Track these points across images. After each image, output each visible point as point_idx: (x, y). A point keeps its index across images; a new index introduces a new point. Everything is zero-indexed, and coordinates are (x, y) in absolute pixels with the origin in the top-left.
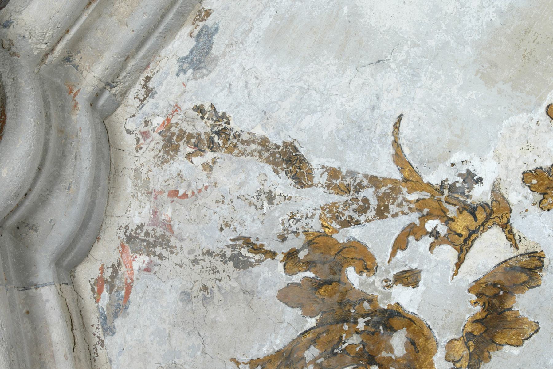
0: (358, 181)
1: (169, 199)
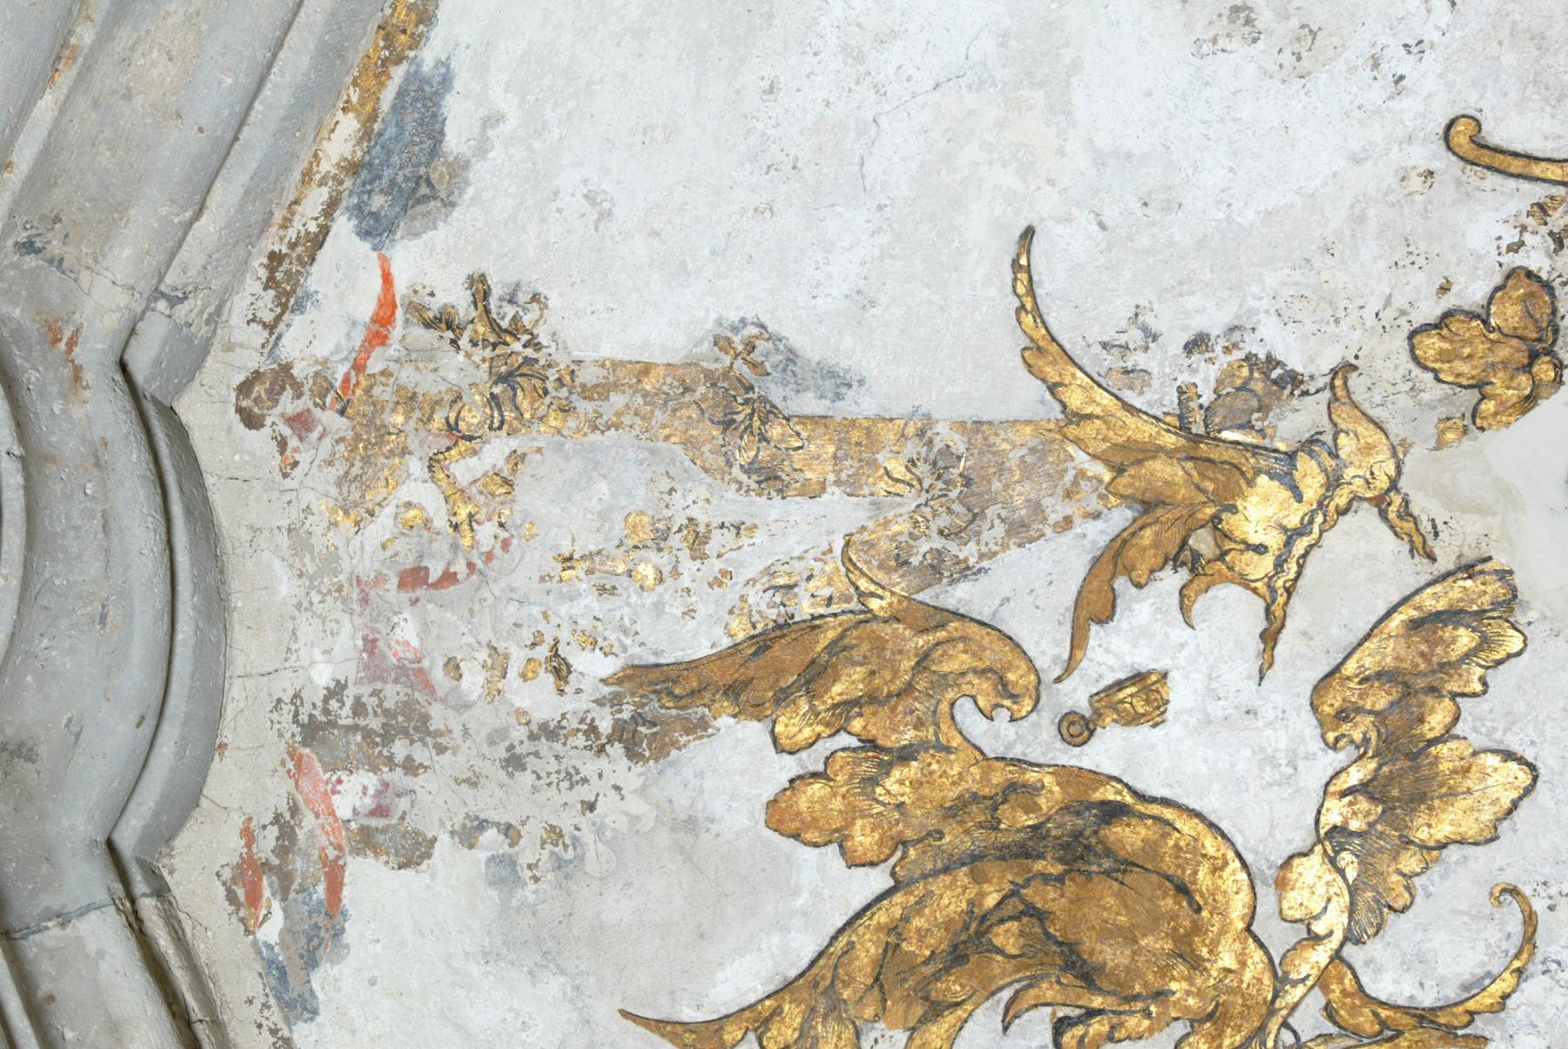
0: (938, 445)
1: (405, 596)
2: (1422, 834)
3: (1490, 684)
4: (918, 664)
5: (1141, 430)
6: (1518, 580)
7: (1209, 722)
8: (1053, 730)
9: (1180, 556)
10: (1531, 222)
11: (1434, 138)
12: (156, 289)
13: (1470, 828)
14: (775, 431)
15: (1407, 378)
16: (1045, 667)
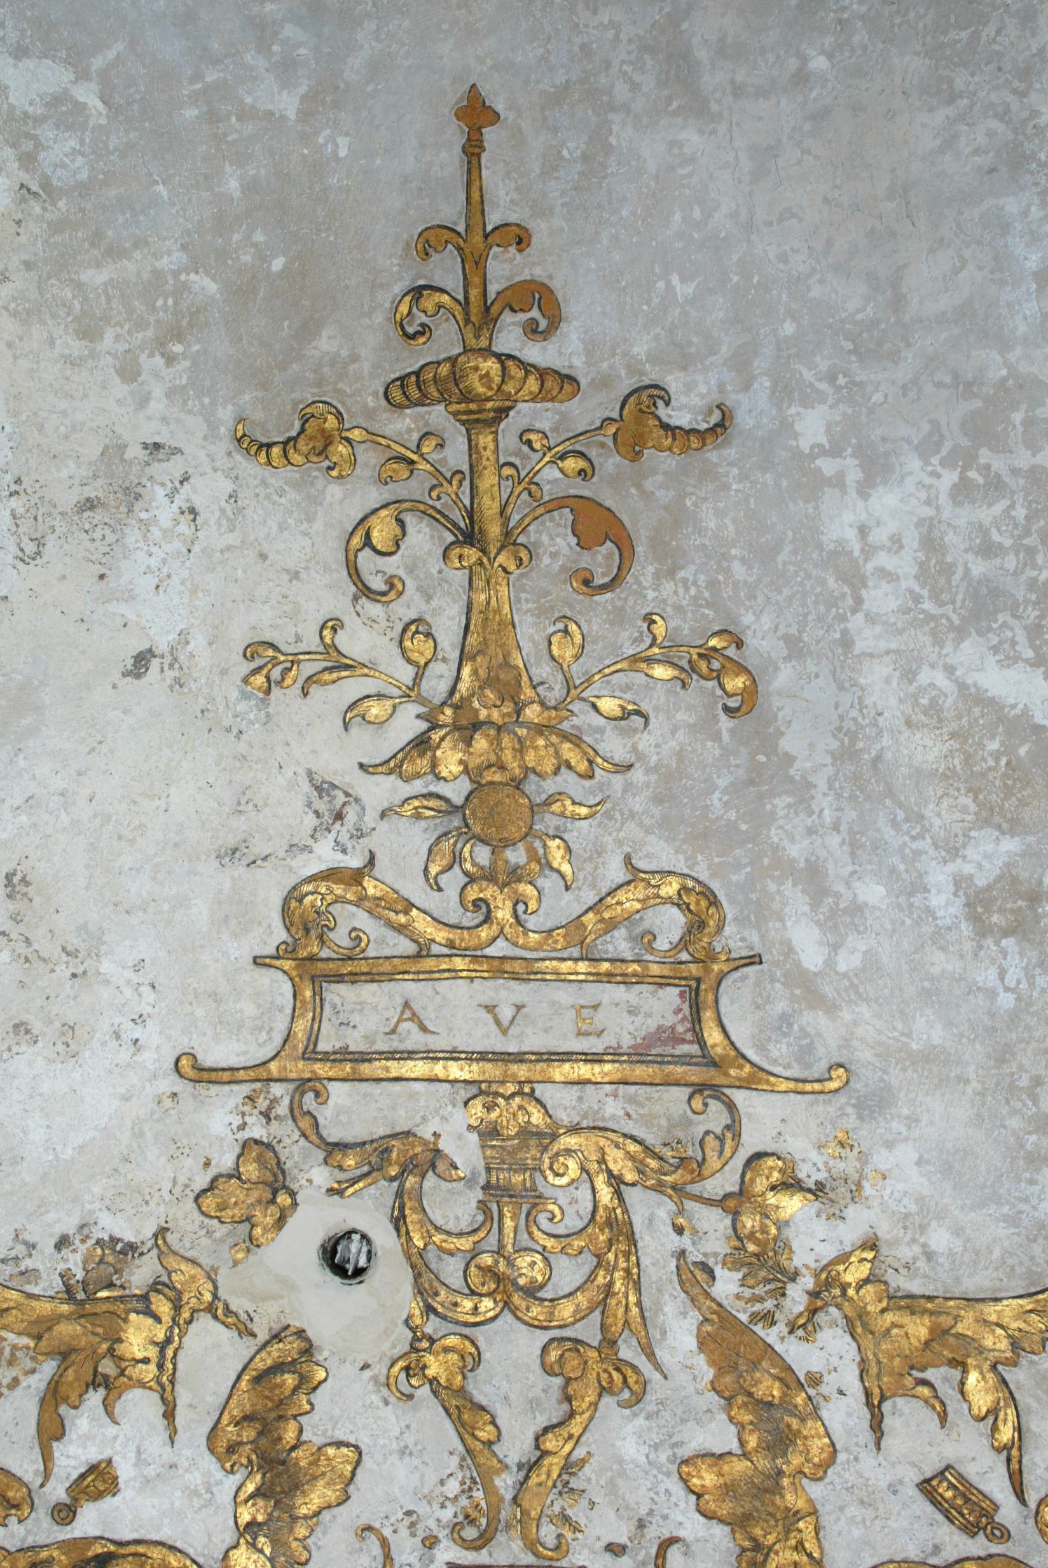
2: (304, 1511)
5: (45, 1308)
6: (310, 1334)
7: (148, 1481)
8: (49, 1518)
9: (97, 1381)
10: (247, 1109)
13: (332, 1495)
15: (202, 1227)
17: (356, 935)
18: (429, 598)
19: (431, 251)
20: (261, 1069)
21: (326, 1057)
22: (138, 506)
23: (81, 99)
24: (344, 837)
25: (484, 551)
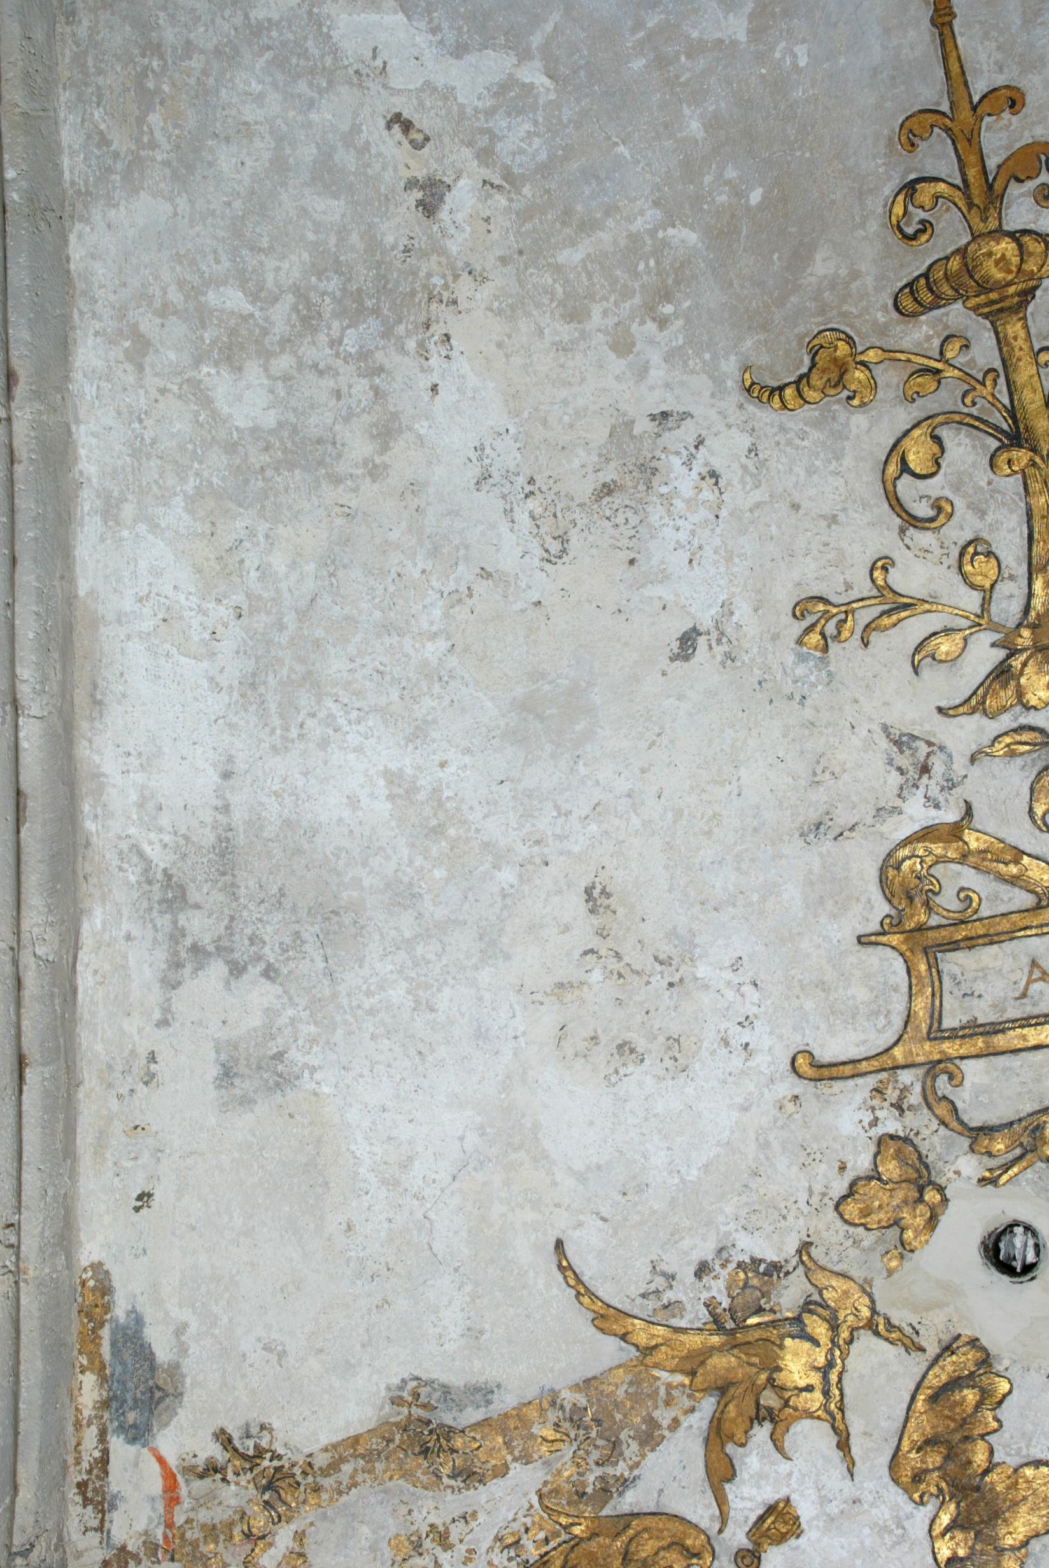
0: (568, 1407)
2: (1009, 1541)
3: (1002, 1419)
4: (624, 1559)
5: (695, 1341)
6: (984, 1342)
7: (832, 1520)
10: (876, 1102)
11: (786, 1074)
12: (10, 1554)
14: (458, 1443)
15: (847, 1236)
16: (708, 1526)
17: (965, 895)
18: (982, 514)
19: (916, 140)
20: (885, 1057)
21: (953, 1035)
22: (656, 481)
23: (527, 80)
24: (934, 791)
25: (1034, 450)
